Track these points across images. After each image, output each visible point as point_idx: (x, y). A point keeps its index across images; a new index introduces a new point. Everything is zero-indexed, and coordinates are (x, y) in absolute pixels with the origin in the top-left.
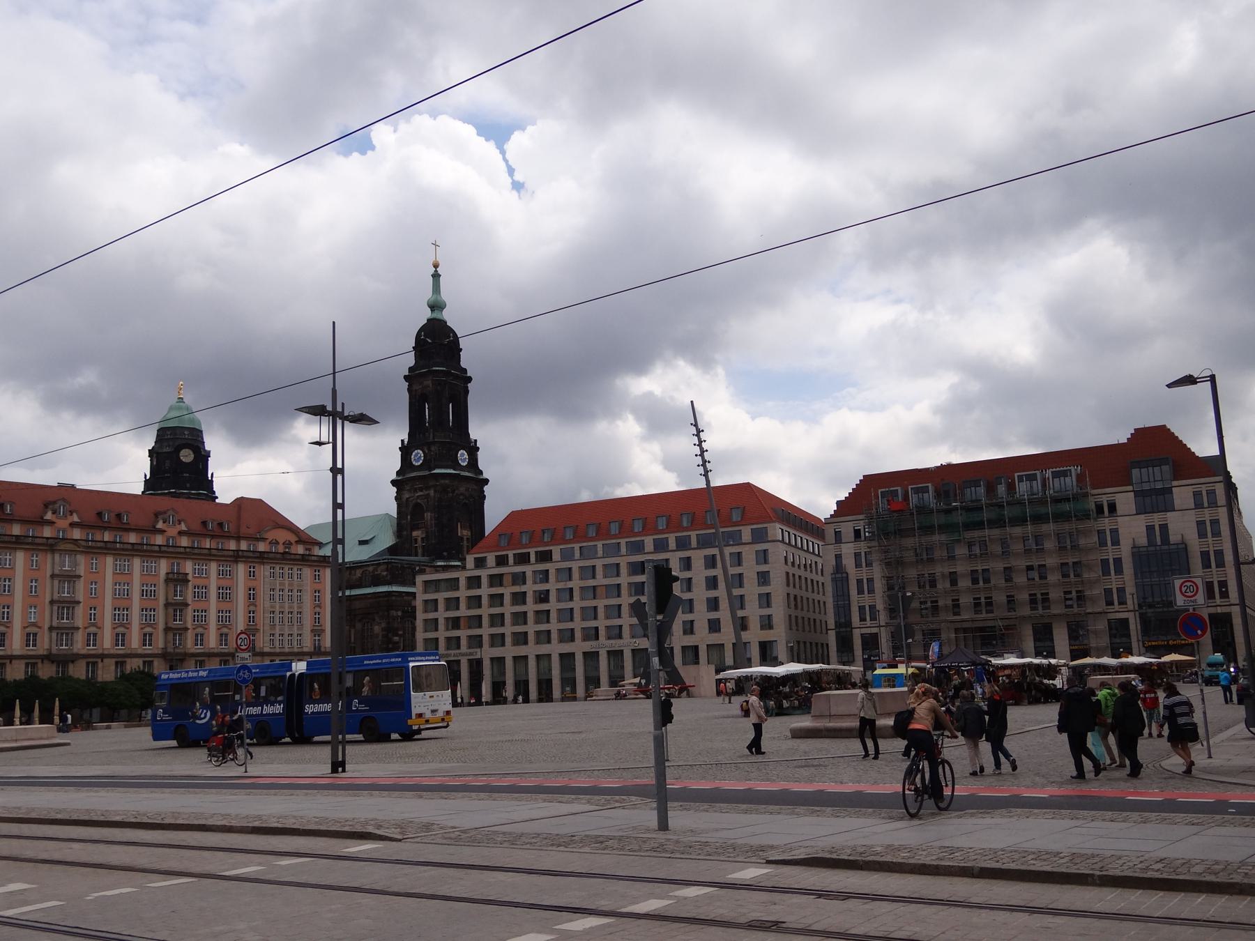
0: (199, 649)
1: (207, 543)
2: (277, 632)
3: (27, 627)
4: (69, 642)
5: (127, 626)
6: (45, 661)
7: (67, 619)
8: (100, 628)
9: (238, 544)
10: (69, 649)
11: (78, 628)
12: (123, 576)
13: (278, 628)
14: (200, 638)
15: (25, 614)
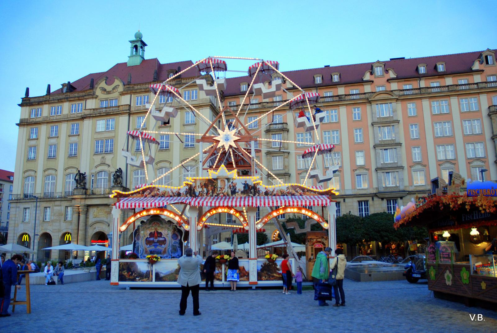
3: (356, 170)
6: (375, 199)
15: (353, 159)
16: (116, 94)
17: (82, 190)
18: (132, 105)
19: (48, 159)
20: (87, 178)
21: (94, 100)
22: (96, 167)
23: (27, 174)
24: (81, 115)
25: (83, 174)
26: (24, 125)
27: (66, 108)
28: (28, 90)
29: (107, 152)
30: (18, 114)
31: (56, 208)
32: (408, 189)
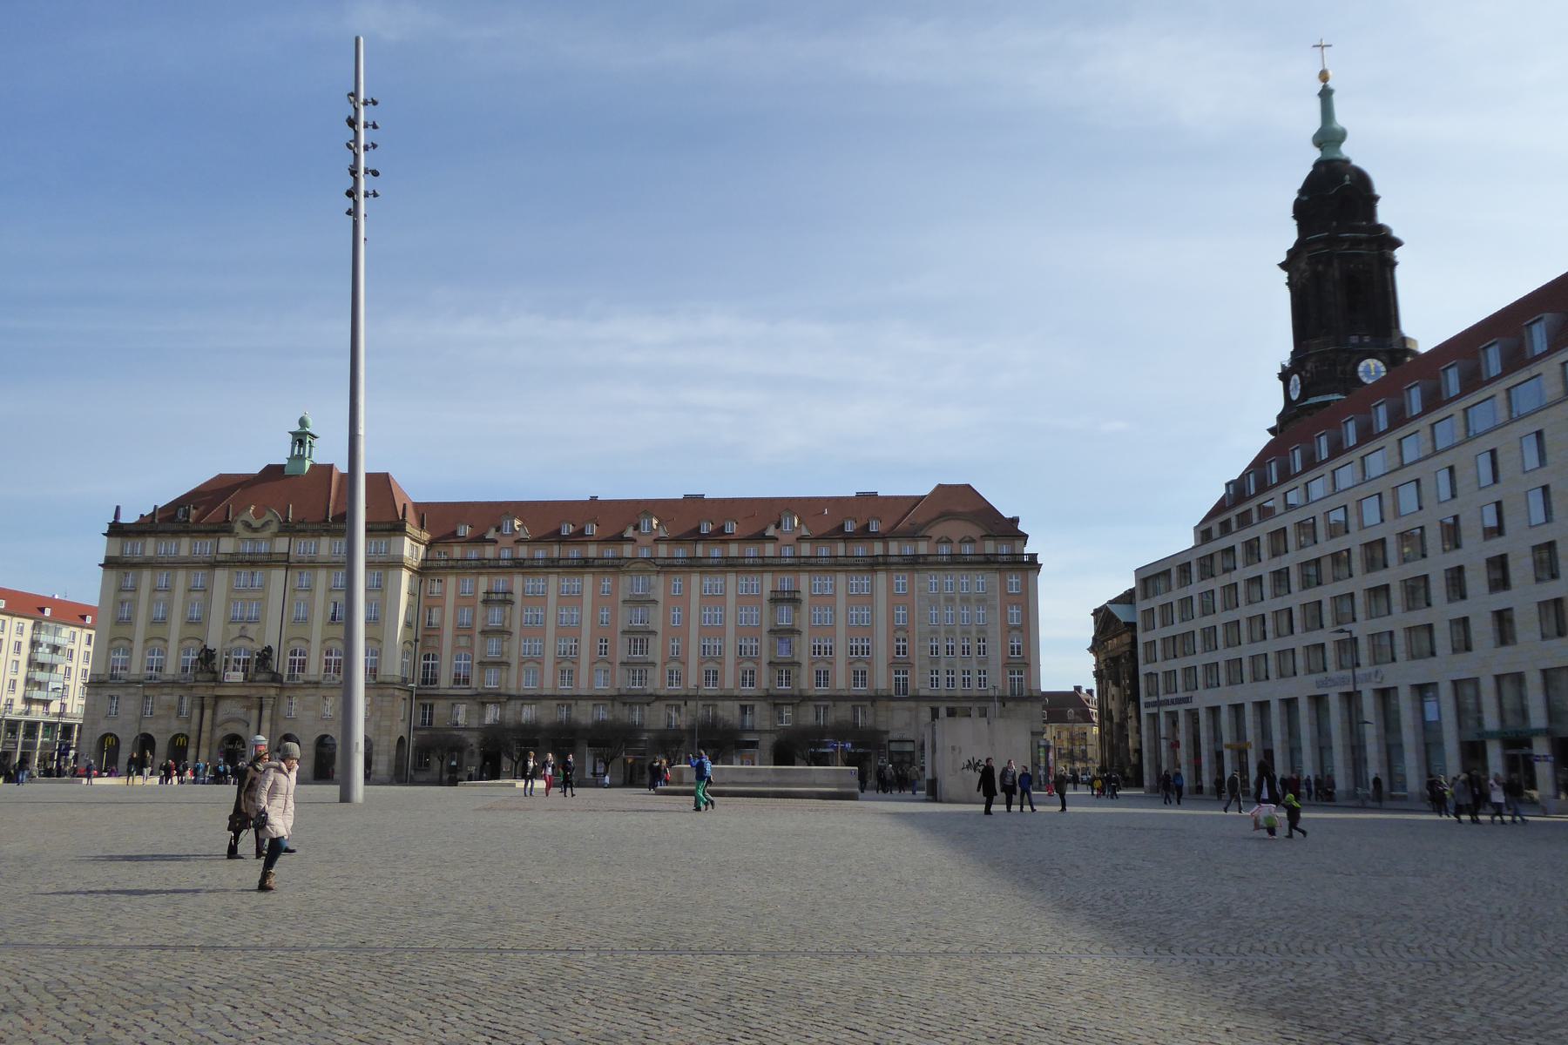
0: (822, 690)
1: (840, 549)
2: (943, 667)
3: (596, 663)
4: (644, 681)
5: (720, 660)
7: (642, 653)
8: (683, 663)
9: (886, 548)
10: (643, 689)
11: (653, 664)
12: (714, 599)
13: (943, 663)
14: (823, 677)
16: (267, 533)
17: (209, 675)
18: (291, 553)
19: (153, 622)
20: (218, 656)
21: (232, 539)
22: (232, 641)
23: (116, 643)
24: (208, 559)
25: (211, 651)
26: (112, 568)
27: (184, 547)
28: (118, 508)
29: (250, 621)
30: (100, 548)
31: (163, 697)
32: (658, 693)
